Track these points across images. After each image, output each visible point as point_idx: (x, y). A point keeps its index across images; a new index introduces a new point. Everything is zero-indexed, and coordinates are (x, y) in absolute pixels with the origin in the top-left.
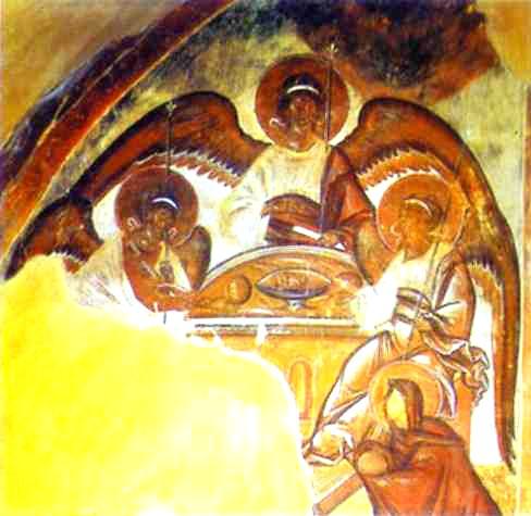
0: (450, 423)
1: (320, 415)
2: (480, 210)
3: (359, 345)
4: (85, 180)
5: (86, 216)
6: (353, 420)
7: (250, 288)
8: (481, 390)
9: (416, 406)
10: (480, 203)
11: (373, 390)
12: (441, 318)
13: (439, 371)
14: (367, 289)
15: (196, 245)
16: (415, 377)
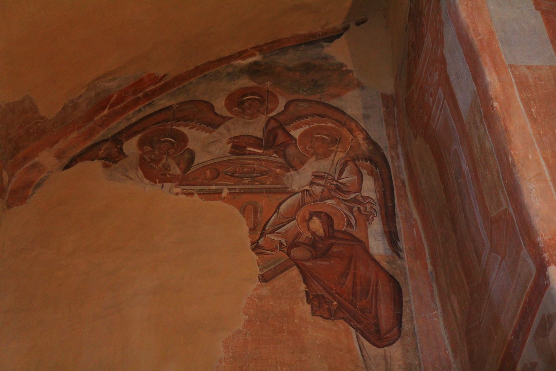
0: (354, 233)
1: (264, 229)
2: (360, 139)
3: (289, 196)
4: (120, 133)
5: (119, 146)
6: (286, 232)
7: (219, 173)
8: (371, 216)
9: (328, 220)
10: (360, 137)
11: (299, 216)
12: (342, 184)
13: (342, 207)
14: (292, 172)
15: (187, 156)
16: (328, 210)
